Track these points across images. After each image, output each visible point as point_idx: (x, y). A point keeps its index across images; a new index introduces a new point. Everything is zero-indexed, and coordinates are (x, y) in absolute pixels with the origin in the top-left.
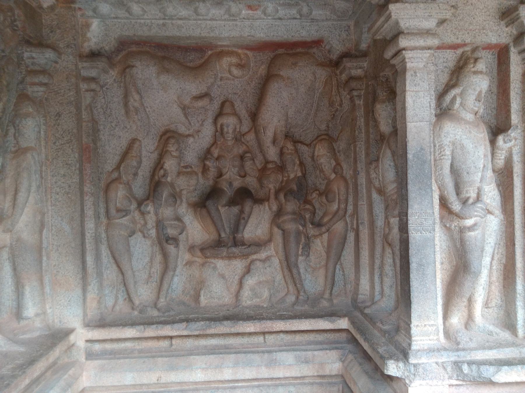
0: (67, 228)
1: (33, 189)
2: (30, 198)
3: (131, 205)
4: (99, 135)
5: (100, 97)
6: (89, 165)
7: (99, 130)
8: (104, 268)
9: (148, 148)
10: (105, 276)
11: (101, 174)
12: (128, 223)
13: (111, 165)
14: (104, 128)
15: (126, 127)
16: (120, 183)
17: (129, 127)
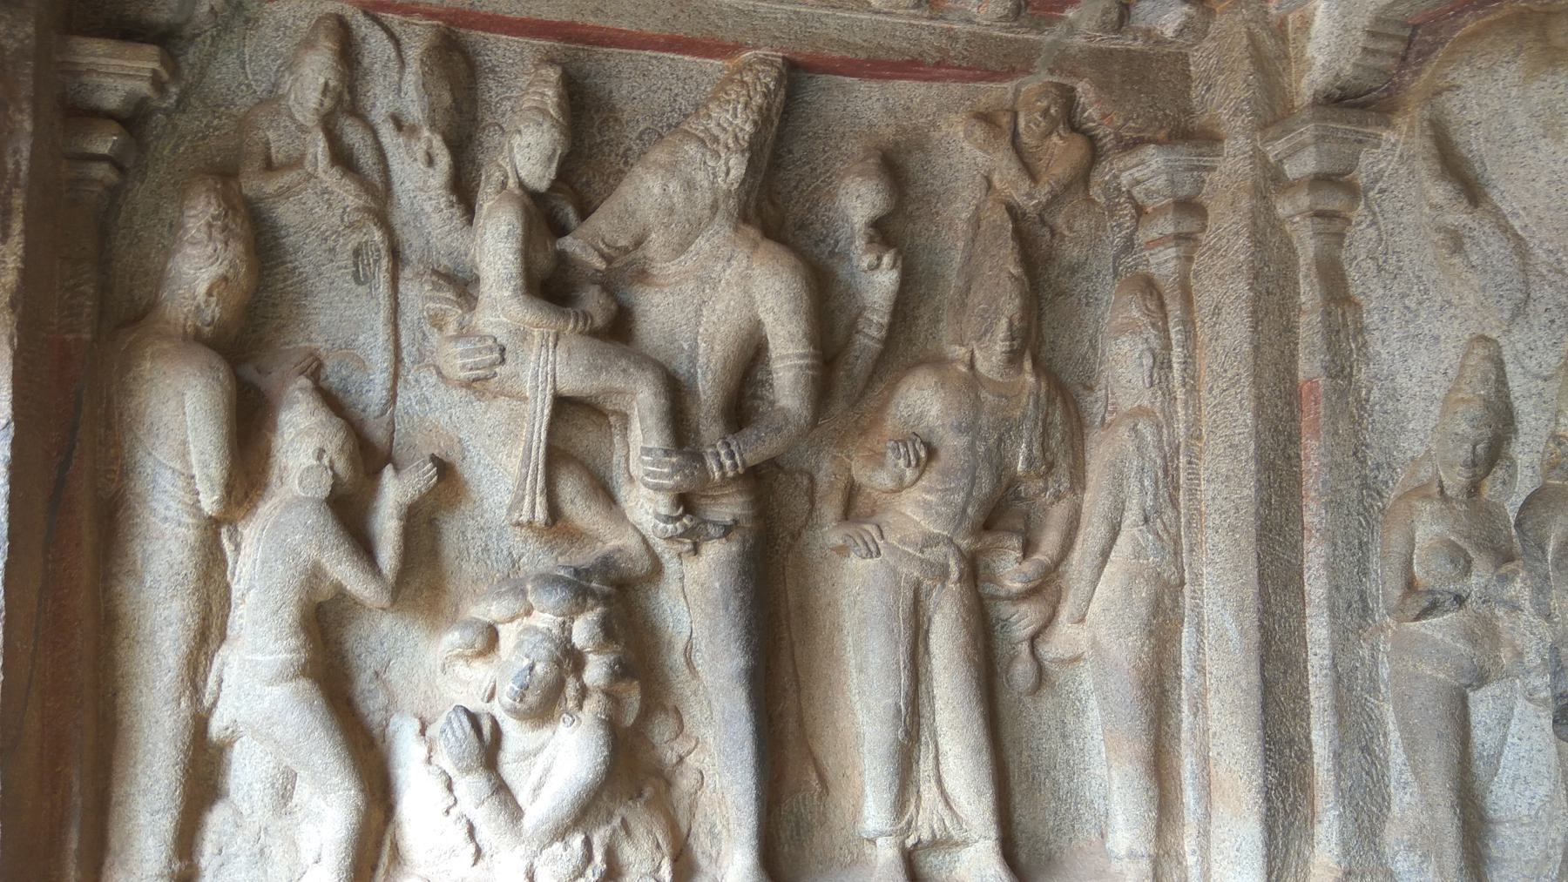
0: (1233, 632)
1: (1132, 516)
2: (1121, 540)
3: (1467, 571)
4: (1365, 344)
5: (1359, 224)
6: (1315, 443)
7: (1361, 330)
8: (1393, 783)
9: (1532, 365)
10: (1395, 809)
11: (1378, 467)
12: (1448, 639)
13: (1421, 436)
14: (1383, 319)
15: (1449, 302)
16: (1427, 497)
17: (1455, 301)
